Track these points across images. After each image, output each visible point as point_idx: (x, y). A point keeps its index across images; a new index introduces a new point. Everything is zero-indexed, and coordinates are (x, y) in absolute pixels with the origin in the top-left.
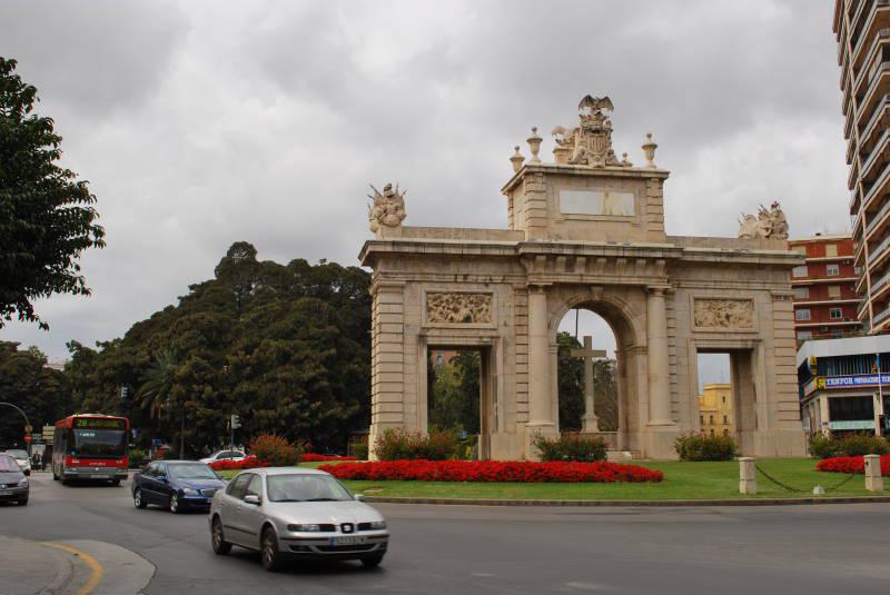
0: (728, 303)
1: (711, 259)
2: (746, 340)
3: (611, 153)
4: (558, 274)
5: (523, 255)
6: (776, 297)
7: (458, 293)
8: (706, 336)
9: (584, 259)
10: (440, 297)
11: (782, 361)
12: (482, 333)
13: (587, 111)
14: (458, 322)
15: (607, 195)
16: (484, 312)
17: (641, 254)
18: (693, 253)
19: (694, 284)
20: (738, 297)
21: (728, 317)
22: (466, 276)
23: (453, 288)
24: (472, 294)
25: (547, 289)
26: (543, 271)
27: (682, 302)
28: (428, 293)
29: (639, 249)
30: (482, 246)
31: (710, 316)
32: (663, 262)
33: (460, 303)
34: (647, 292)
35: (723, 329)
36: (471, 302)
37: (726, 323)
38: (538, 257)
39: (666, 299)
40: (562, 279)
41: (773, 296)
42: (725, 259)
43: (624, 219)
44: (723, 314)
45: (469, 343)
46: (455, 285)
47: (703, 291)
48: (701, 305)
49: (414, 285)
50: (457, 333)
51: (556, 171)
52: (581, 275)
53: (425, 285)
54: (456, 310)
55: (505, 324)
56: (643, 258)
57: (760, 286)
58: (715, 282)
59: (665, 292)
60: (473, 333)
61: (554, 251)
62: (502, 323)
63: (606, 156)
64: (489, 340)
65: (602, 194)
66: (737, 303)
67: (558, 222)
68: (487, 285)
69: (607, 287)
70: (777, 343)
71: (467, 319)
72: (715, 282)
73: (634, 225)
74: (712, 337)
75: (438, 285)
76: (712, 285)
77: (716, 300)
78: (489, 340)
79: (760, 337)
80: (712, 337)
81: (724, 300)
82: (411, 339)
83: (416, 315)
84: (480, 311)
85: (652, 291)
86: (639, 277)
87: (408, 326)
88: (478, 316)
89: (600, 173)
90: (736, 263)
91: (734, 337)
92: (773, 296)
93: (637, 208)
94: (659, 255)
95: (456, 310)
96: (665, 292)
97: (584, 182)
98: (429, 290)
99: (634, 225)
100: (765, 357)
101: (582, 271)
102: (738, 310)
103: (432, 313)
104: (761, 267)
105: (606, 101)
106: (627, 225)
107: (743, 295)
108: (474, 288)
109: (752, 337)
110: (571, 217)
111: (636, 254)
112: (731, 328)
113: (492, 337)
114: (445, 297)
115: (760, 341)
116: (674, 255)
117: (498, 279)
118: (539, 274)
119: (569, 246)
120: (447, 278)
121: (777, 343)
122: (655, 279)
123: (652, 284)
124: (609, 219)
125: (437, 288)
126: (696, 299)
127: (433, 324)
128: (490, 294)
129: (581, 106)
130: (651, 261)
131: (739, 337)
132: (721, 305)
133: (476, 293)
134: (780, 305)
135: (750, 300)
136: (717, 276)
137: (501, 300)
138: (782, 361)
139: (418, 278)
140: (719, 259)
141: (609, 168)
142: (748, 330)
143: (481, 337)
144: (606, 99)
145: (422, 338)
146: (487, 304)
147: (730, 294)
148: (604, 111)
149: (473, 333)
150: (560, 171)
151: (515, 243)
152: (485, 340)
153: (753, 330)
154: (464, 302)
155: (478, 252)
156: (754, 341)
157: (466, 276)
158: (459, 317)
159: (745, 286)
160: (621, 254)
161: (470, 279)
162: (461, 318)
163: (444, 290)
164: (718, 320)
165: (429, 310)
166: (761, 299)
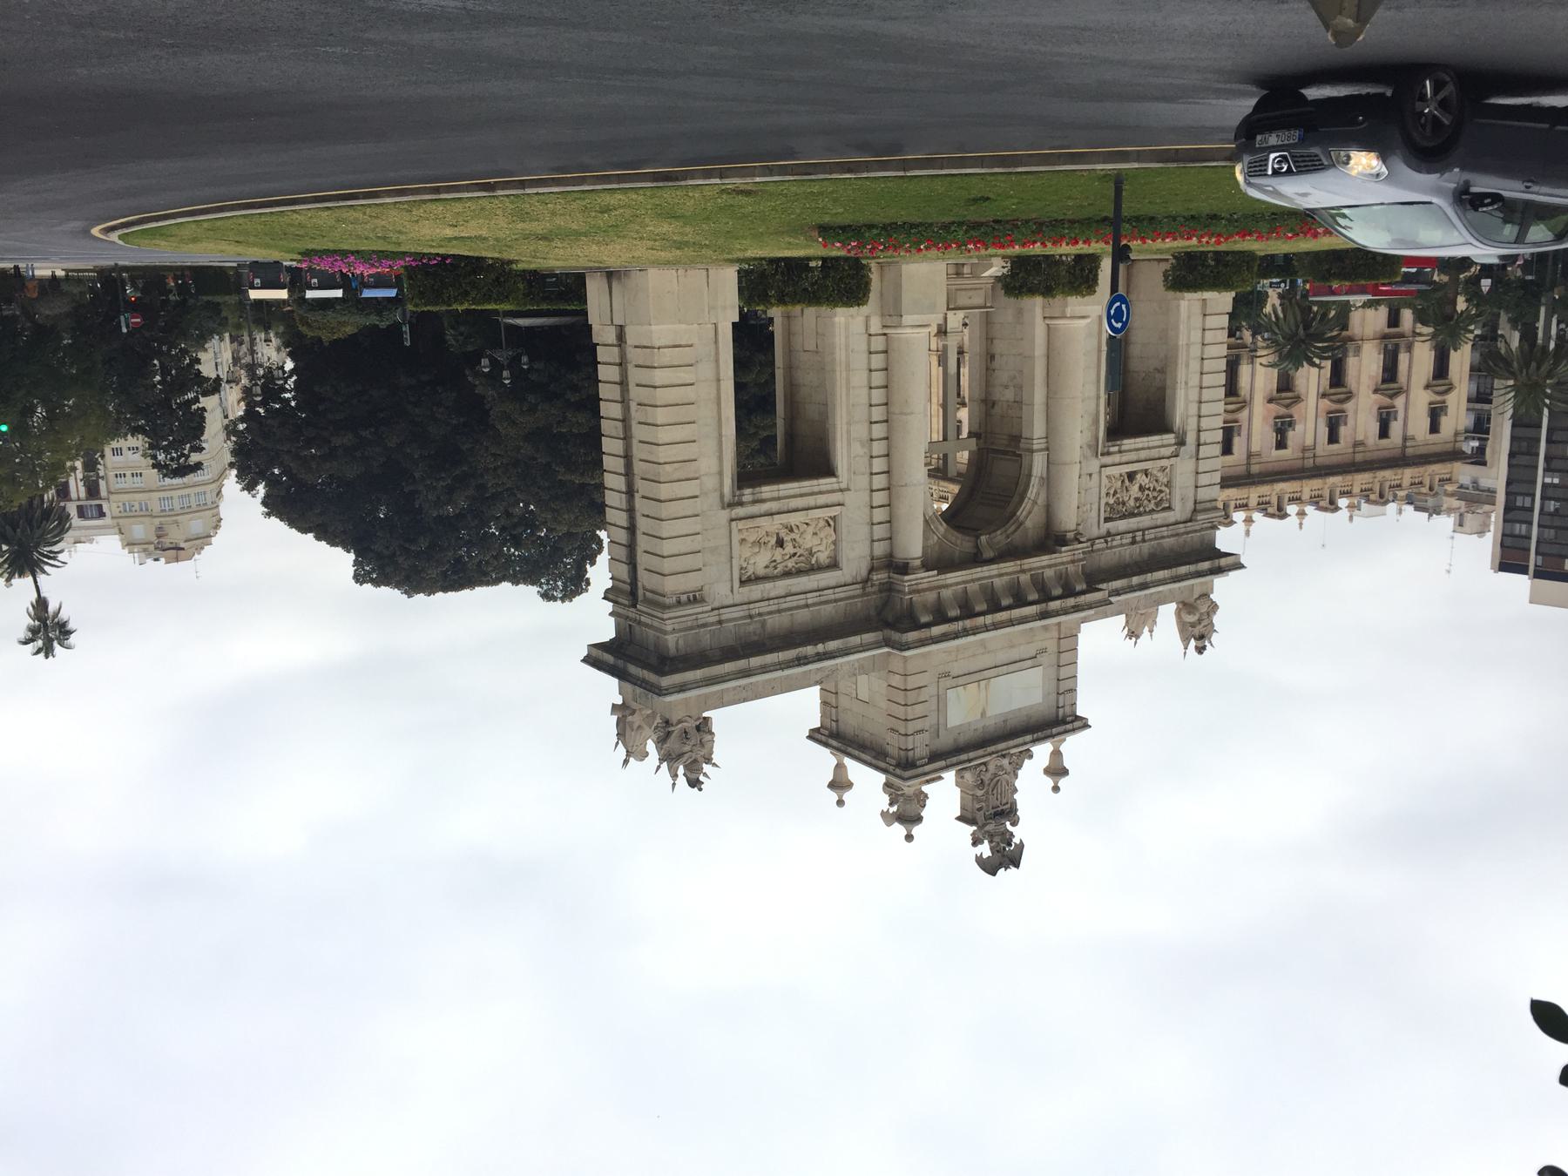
0: (780, 568)
1: (832, 645)
2: (755, 502)
4: (1050, 566)
6: (695, 599)
7: (1140, 514)
8: (822, 499)
9: (1005, 602)
10: (1157, 505)
11: (688, 471)
12: (1117, 458)
14: (1141, 471)
15: (983, 714)
16: (1112, 492)
17: (959, 625)
19: (841, 593)
20: (768, 585)
21: (780, 543)
22: (1134, 542)
23: (1145, 521)
24: (1123, 517)
26: (1071, 568)
27: (856, 558)
28: (1169, 508)
29: (966, 632)
30: (1132, 589)
31: (809, 541)
32: (925, 619)
33: (1137, 499)
34: (939, 562)
35: (794, 519)
36: (1124, 503)
37: (783, 533)
38: (1084, 587)
39: (890, 555)
40: (1044, 560)
41: (702, 600)
42: (809, 650)
43: (961, 681)
44: (789, 549)
45: (1145, 439)
46: (1141, 526)
47: (823, 584)
48: (823, 557)
49: (1184, 518)
50: (1143, 455)
51: (1054, 731)
52: (1023, 571)
53: (1172, 520)
54: (1141, 488)
55: (1090, 475)
56: (956, 619)
57: (727, 614)
58: (807, 606)
59: (904, 569)
60: (1125, 458)
61: (1071, 602)
62: (1095, 477)
63: (987, 777)
64: (1112, 449)
65: (989, 714)
66: (761, 572)
67: (1043, 651)
68: (1109, 534)
69: (976, 560)
70: (696, 506)
71: (1131, 476)
72: (807, 606)
73: (947, 675)
74: (811, 501)
75: (1159, 522)
76: (812, 598)
77: (799, 572)
78: (1112, 449)
79: (725, 515)
80: (811, 501)
81: (787, 574)
82: (1191, 439)
83: (1183, 468)
84: (1115, 492)
85: (926, 566)
86: (946, 586)
87: (1191, 458)
88: (1120, 483)
90: (771, 651)
91: (773, 506)
92: (702, 600)
93: (941, 701)
94: (936, 630)
95: (1141, 488)
99: (947, 675)
100: (721, 473)
102: (760, 561)
103: (1165, 480)
104: (730, 654)
106: (954, 673)
107: (756, 591)
108: (1122, 525)
109: (740, 511)
110: (1029, 663)
111: (968, 623)
112: (773, 525)
113: (1109, 453)
114: (1152, 506)
115: (731, 505)
116: (912, 636)
117: (1100, 544)
118: (1073, 562)
119: (1056, 613)
120: (1150, 535)
121: (696, 506)
122: (922, 585)
124: (978, 675)
125: (1160, 518)
126: (834, 565)
127: (1164, 463)
128: (1107, 520)
129: (1021, 846)
130: (941, 617)
131: (765, 507)
132: (791, 564)
133: (1121, 518)
134: (689, 583)
135: (743, 583)
136: (803, 616)
137: (1094, 514)
138: (688, 471)
139: (1181, 528)
140: (820, 648)
142: (750, 523)
143: (1120, 452)
144: (993, 873)
145: (1181, 442)
146: (1107, 504)
147: (781, 586)
149: (1125, 458)
150: (1048, 732)
152: (1116, 449)
153: (741, 524)
154: (1132, 503)
155: (1135, 580)
156: (741, 504)
157: (1134, 542)
158: (1140, 478)
159: (757, 608)
160: (989, 619)
161: (1127, 539)
162: (1138, 476)
163: (1155, 516)
164: (793, 536)
165: (1168, 485)
166: (722, 590)
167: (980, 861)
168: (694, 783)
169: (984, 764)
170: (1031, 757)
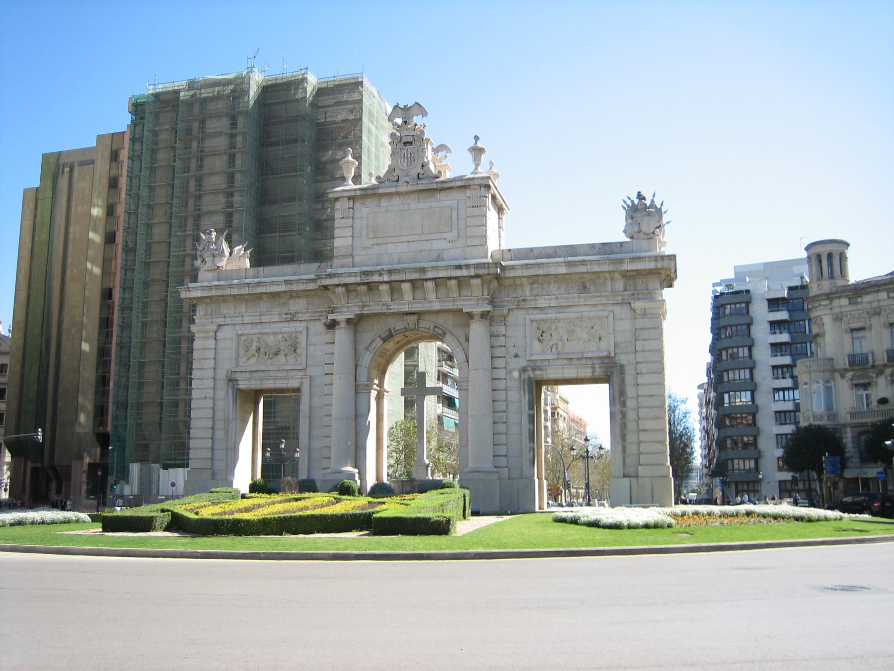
25: (349, 321)
85: (470, 315)
98: (240, 332)
105: (419, 109)
167: (424, 113)
168: (640, 197)
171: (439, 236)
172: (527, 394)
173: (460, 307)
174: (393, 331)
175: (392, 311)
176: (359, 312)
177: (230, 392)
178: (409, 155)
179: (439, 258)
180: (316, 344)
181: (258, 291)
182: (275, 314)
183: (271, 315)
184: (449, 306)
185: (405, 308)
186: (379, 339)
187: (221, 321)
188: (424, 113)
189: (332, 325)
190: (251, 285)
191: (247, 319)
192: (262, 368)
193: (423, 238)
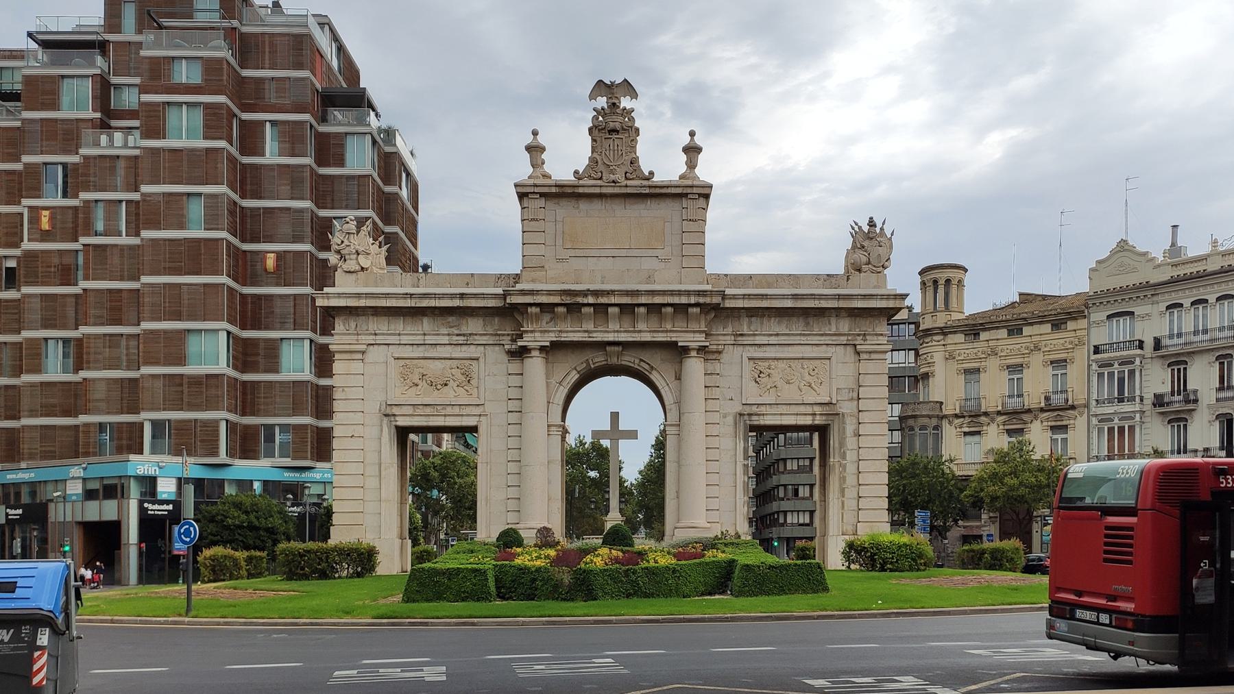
3: (634, 162)
5: (514, 306)
13: (602, 102)
18: (734, 297)
25: (542, 349)
85: (686, 350)
89: (617, 190)
96: (702, 350)
97: (597, 205)
101: (591, 327)
105: (628, 88)
123: (683, 339)
129: (593, 96)
141: (629, 183)
148: (626, 103)
151: (500, 291)
167: (634, 94)
169: (626, 178)
170: (576, 172)
171: (650, 253)
172: (742, 441)
173: (674, 339)
174: (591, 362)
175: (594, 339)
176: (555, 339)
177: (385, 429)
178: (616, 148)
179: (650, 279)
180: (495, 375)
181: (424, 305)
182: (443, 335)
183: (438, 335)
184: (661, 337)
185: (611, 337)
186: (574, 372)
187: (371, 339)
188: (634, 94)
189: (521, 353)
190: (414, 296)
191: (405, 339)
192: (427, 401)
193: (631, 253)
